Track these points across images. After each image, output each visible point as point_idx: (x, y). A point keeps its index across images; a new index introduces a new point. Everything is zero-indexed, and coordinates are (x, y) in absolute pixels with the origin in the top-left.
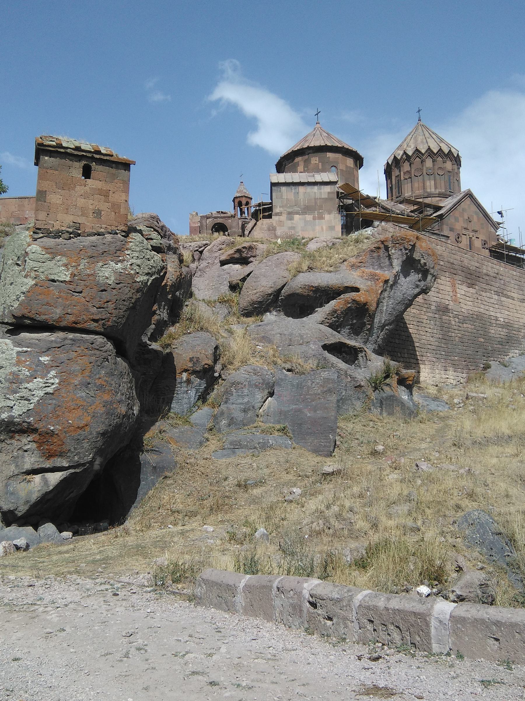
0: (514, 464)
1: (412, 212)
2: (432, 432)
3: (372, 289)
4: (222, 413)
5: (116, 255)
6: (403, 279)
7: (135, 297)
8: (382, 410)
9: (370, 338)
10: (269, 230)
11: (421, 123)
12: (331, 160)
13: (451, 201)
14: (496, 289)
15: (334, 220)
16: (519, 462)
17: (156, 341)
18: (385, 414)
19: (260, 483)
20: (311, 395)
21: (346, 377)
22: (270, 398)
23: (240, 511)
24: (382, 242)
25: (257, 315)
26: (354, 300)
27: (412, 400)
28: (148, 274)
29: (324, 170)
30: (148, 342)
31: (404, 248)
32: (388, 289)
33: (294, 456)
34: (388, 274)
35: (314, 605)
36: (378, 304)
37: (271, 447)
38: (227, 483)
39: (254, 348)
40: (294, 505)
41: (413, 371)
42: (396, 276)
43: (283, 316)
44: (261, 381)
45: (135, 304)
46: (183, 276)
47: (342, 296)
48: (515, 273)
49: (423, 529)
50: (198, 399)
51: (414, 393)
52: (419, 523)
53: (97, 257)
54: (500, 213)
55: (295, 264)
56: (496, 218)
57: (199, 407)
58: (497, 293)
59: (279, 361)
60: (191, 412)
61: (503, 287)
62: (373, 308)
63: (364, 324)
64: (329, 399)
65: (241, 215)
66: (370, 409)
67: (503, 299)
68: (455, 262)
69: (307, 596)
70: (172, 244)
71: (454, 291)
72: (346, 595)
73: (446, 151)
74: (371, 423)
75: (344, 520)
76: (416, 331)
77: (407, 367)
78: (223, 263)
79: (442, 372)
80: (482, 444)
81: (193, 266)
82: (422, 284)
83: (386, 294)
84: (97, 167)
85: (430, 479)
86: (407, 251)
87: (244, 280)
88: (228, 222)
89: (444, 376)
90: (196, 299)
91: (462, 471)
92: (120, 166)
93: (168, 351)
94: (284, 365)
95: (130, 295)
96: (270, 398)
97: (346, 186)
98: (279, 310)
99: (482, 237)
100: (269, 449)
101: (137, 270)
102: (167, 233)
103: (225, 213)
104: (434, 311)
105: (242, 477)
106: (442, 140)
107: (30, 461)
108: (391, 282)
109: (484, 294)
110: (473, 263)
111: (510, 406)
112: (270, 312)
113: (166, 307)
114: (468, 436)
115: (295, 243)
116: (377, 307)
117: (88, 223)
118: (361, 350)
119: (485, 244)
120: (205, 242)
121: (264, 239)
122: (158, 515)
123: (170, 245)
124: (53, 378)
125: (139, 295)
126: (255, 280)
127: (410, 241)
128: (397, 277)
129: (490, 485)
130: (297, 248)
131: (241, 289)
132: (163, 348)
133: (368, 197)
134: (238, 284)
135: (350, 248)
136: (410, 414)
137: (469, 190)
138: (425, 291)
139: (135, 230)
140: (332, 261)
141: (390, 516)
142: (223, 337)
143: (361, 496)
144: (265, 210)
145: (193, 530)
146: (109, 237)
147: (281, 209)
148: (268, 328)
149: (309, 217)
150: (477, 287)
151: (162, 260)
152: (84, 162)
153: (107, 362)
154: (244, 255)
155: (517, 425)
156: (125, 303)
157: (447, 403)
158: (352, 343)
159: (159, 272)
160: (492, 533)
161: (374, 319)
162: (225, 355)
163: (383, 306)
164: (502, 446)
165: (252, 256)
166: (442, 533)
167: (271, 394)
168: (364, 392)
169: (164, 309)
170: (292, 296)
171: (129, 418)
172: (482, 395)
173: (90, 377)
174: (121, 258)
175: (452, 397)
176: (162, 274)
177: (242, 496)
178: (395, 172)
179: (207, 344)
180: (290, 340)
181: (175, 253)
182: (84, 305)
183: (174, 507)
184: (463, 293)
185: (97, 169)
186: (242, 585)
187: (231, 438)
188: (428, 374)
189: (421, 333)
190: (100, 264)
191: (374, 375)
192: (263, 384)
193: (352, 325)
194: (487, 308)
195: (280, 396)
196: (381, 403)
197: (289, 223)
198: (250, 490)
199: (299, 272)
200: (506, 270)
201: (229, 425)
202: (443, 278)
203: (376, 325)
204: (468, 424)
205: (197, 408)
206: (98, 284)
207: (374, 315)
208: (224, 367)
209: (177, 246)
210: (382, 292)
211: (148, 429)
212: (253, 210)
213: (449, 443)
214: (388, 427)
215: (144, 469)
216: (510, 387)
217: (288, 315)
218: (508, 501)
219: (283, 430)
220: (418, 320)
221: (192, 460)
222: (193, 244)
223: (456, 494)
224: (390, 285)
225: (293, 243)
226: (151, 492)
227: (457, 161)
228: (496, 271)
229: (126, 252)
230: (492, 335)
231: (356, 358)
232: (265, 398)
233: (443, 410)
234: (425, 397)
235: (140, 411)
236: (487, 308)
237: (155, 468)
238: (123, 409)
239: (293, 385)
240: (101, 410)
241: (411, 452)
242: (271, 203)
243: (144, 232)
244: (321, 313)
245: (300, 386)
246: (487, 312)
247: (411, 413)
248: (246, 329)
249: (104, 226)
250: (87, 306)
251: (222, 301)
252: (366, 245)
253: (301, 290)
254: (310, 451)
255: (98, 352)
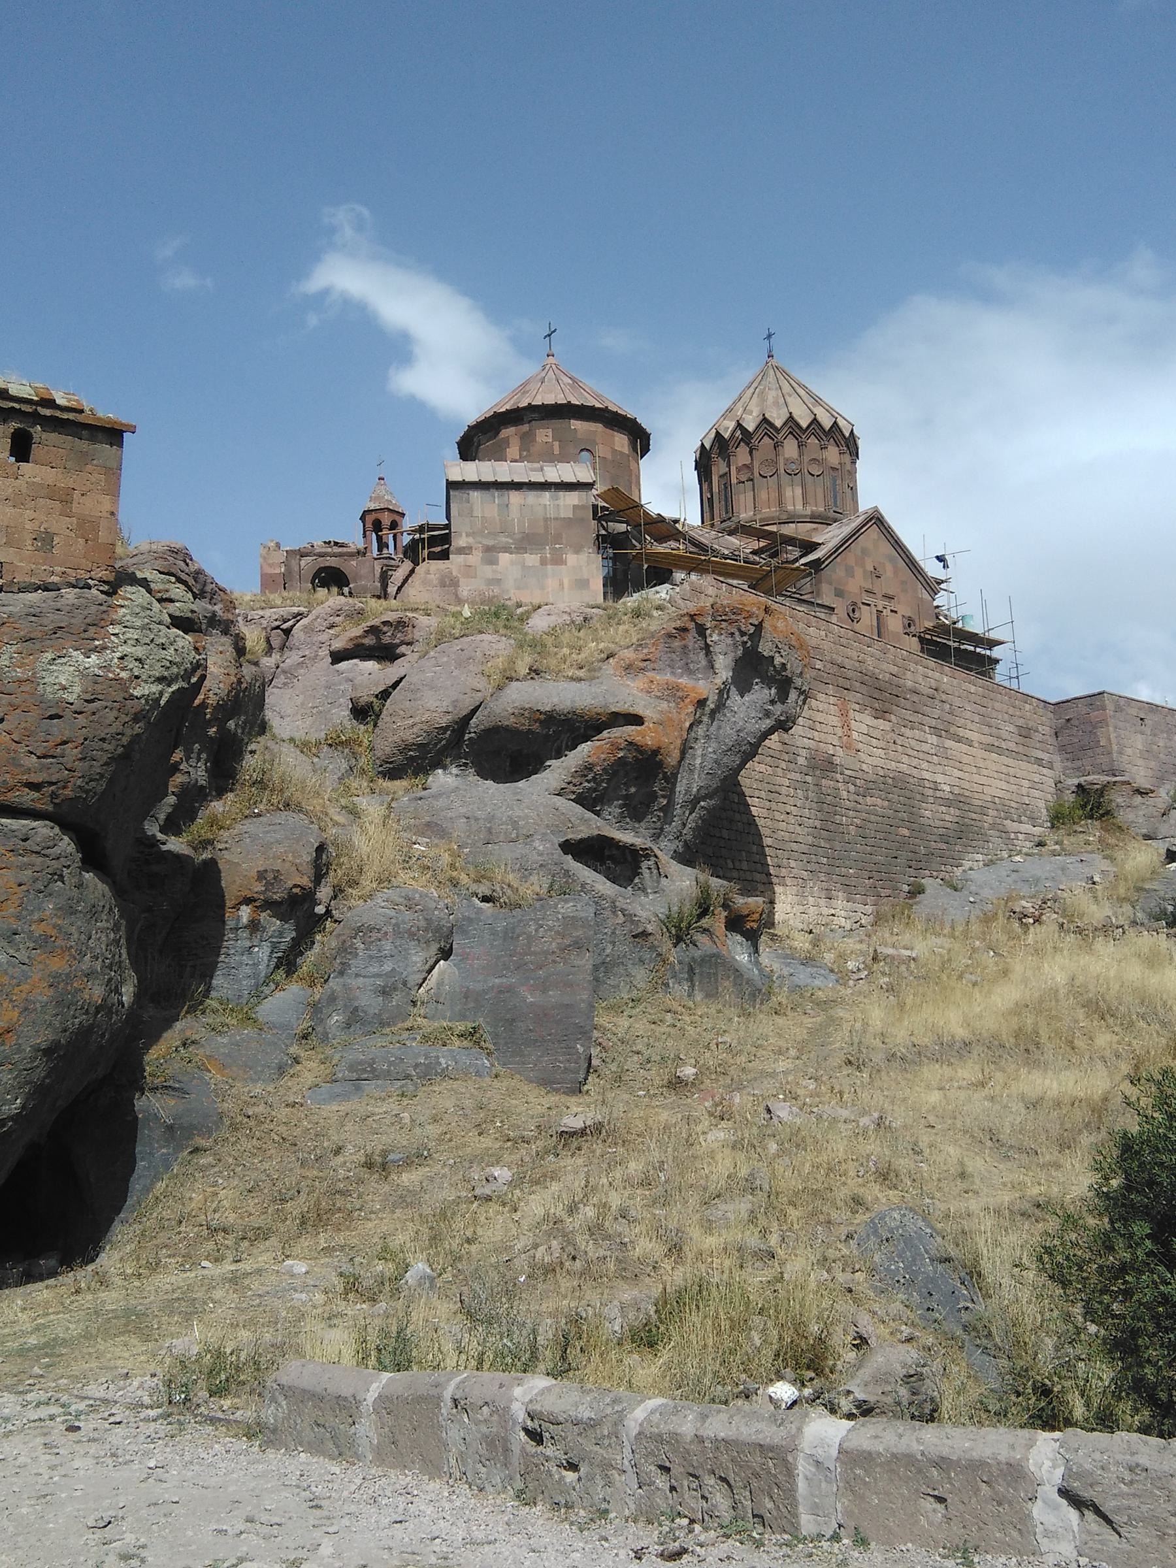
0: (978, 1103)
1: (754, 552)
2: (801, 1034)
3: (670, 719)
4: (332, 999)
5: (86, 635)
6: (738, 698)
7: (129, 732)
8: (692, 986)
9: (667, 828)
10: (443, 585)
11: (774, 362)
12: (579, 436)
13: (837, 532)
14: (934, 723)
15: (590, 567)
16: (986, 1098)
17: (178, 833)
18: (699, 996)
19: (418, 1157)
20: (535, 953)
21: (614, 913)
22: (442, 962)
23: (370, 1225)
24: (692, 617)
25: (416, 774)
26: (631, 743)
27: (757, 963)
28: (160, 680)
29: (564, 458)
30: (160, 836)
31: (739, 630)
32: (705, 719)
33: (496, 1092)
34: (705, 687)
35: (536, 1436)
36: (683, 753)
37: (445, 1075)
38: (340, 1159)
39: (406, 847)
40: (494, 1207)
41: (760, 900)
42: (721, 692)
43: (473, 778)
44: (423, 924)
45: (129, 748)
46: (244, 686)
47: (605, 734)
48: (973, 689)
49: (781, 1252)
50: (277, 967)
51: (761, 949)
52: (774, 1240)
53: (42, 640)
54: (940, 559)
55: (500, 662)
56: (933, 569)
57: (277, 985)
58: (936, 731)
59: (464, 879)
60: (258, 996)
61: (948, 717)
62: (672, 760)
63: (654, 797)
64: (576, 963)
65: (380, 550)
66: (667, 985)
67: (949, 743)
68: (848, 663)
69: (521, 1416)
70: (220, 613)
71: (846, 725)
72: (609, 1410)
73: (827, 423)
74: (669, 1016)
75: (608, 1237)
76: (764, 813)
77: (746, 892)
78: (338, 657)
79: (823, 902)
80: (908, 1060)
81: (268, 662)
82: (778, 709)
83: (700, 731)
84: (44, 436)
85: (796, 1141)
86: (745, 638)
87: (385, 695)
88: (350, 567)
89: (826, 911)
90: (274, 737)
91: (864, 1121)
92: (100, 436)
93: (206, 855)
94: (473, 887)
95: (117, 727)
96: (442, 962)
97: (614, 493)
98: (465, 765)
99: (904, 610)
100: (439, 1078)
101: (135, 670)
102: (209, 588)
103: (342, 545)
104: (805, 770)
105: (376, 1144)
106: (818, 401)
108: (711, 705)
109: (908, 733)
110: (884, 666)
111: (967, 976)
112: (445, 768)
113: (204, 756)
114: (877, 1043)
115: (501, 615)
116: (682, 758)
118: (647, 854)
119: (909, 625)
120: (295, 610)
121: (432, 606)
122: (177, 1238)
123: (214, 614)
125: (138, 728)
126: (410, 695)
127: (750, 616)
128: (723, 692)
129: (927, 1152)
130: (505, 627)
131: (378, 716)
132: (195, 849)
133: (661, 519)
134: (370, 705)
135: (621, 628)
136: (753, 996)
137: (876, 510)
138: (784, 725)
139: (133, 580)
140: (583, 656)
141: (708, 1226)
142: (336, 824)
143: (646, 1183)
144: (433, 541)
145: (259, 1272)
146: (70, 594)
147: (471, 540)
148: (441, 803)
149: (532, 559)
150: (893, 717)
151: (196, 649)
152: (14, 425)
153: (59, 883)
154: (386, 640)
155: (980, 1017)
156: (106, 746)
157: (832, 971)
158: (626, 837)
159: (187, 676)
160: (932, 1260)
161: (674, 785)
162: (340, 865)
163: (694, 757)
164: (950, 1064)
165: (403, 643)
166: (824, 1261)
167: (446, 954)
168: (653, 948)
169: (199, 760)
170: (494, 732)
171: (110, 1013)
172: (908, 953)
173: (18, 917)
174: (97, 643)
175: (842, 957)
176: (194, 680)
177: (376, 1190)
178: (719, 468)
179: (298, 840)
180: (490, 831)
181: (225, 632)
182: (8, 751)
183: (216, 1220)
184: (865, 730)
185: (44, 440)
186: (372, 1395)
187: (351, 1056)
188: (790, 907)
189: (777, 815)
190: (49, 656)
191: (675, 909)
192: (426, 930)
193: (626, 797)
194: (915, 762)
195: (465, 957)
196: (691, 970)
197: (488, 571)
198: (394, 1176)
199: (510, 679)
200: (955, 682)
201: (348, 1025)
202: (821, 697)
203: (679, 798)
204: (877, 1015)
205: (273, 986)
206: (41, 702)
207: (675, 775)
208: (338, 892)
209: (231, 617)
210: (691, 725)
211: (155, 1038)
212: (406, 539)
213: (837, 1060)
214: (703, 1025)
215: (144, 1133)
216: (966, 934)
217: (483, 774)
218: (965, 1186)
219: (471, 1034)
220: (770, 787)
221: (260, 1109)
222: (267, 613)
223: (852, 1173)
224: (708, 710)
225: (496, 615)
226: (160, 1186)
227: (850, 445)
228: (934, 684)
229: (111, 629)
230: (927, 822)
231: (636, 872)
232: (431, 962)
233: (825, 986)
234: (786, 957)
235: (138, 996)
236: (915, 762)
237: (170, 1128)
238: (96, 992)
239: (494, 933)
240: (43, 996)
241: (755, 1079)
242: (448, 527)
243: (152, 585)
244: (559, 771)
245: (509, 935)
246: (915, 772)
247: (755, 993)
248: (389, 807)
249: (58, 569)
250: (15, 751)
251: (336, 743)
252: (658, 623)
253: (513, 719)
254: (531, 1082)
255: (38, 860)
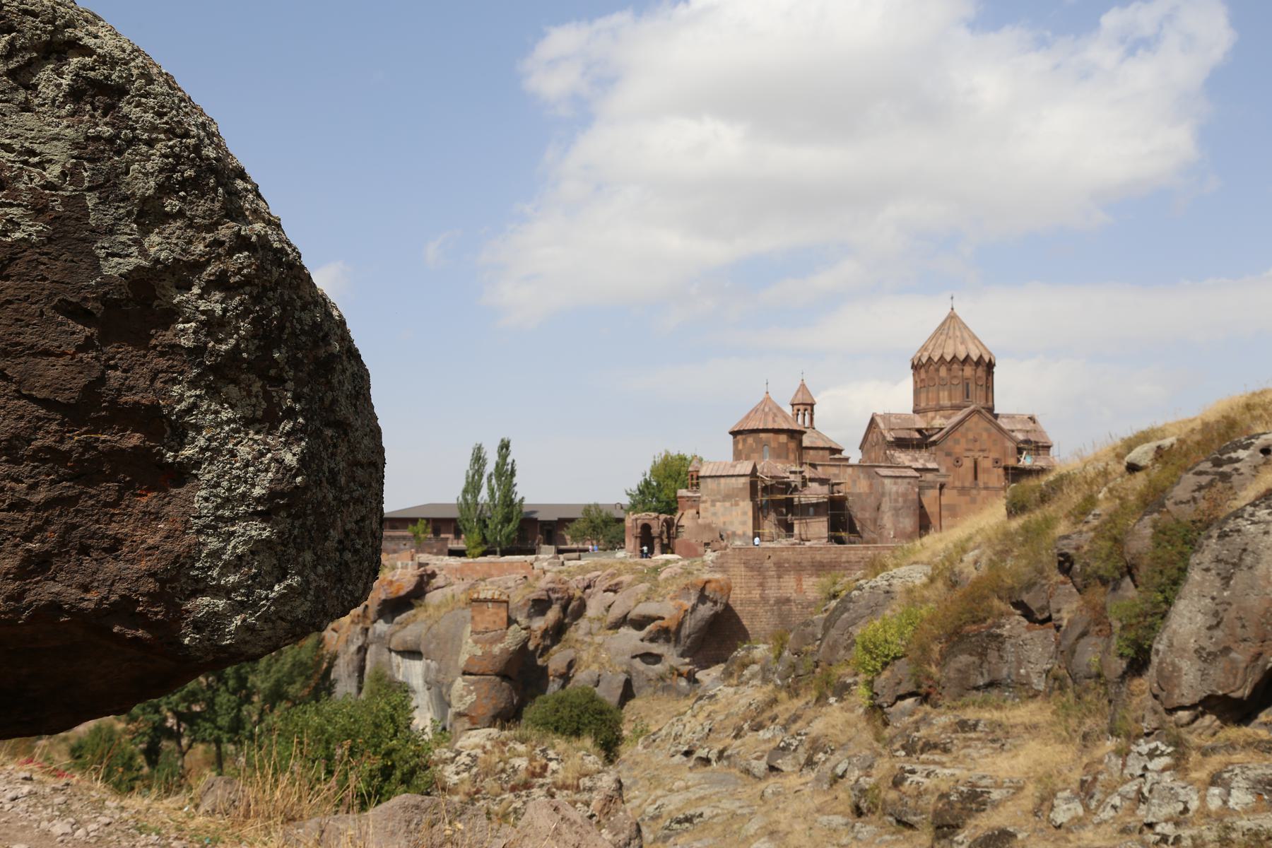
99: (994, 455)
107: (467, 726)
117: (491, 626)
124: (474, 696)
149: (727, 504)
